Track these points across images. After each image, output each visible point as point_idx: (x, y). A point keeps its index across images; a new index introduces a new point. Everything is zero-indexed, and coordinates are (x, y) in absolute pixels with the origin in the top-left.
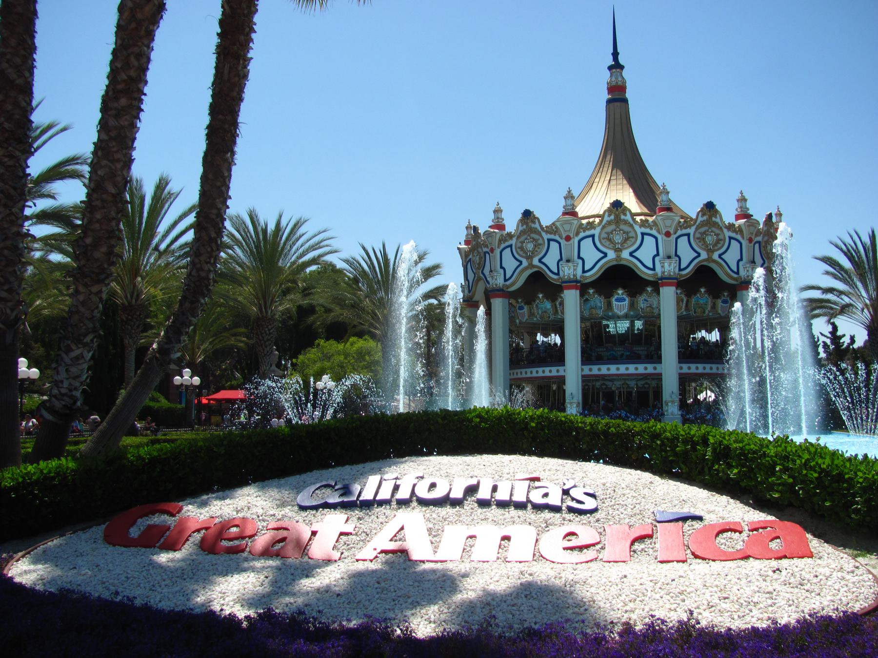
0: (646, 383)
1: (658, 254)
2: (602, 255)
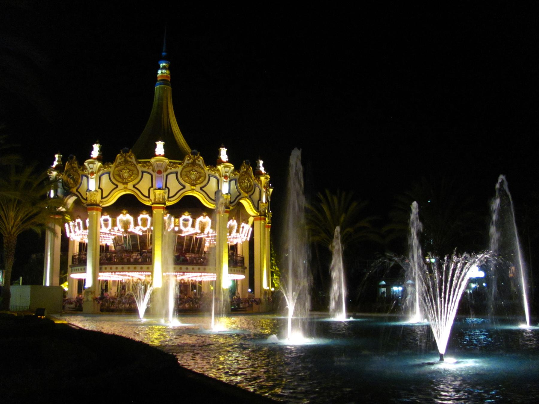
2: (182, 187)
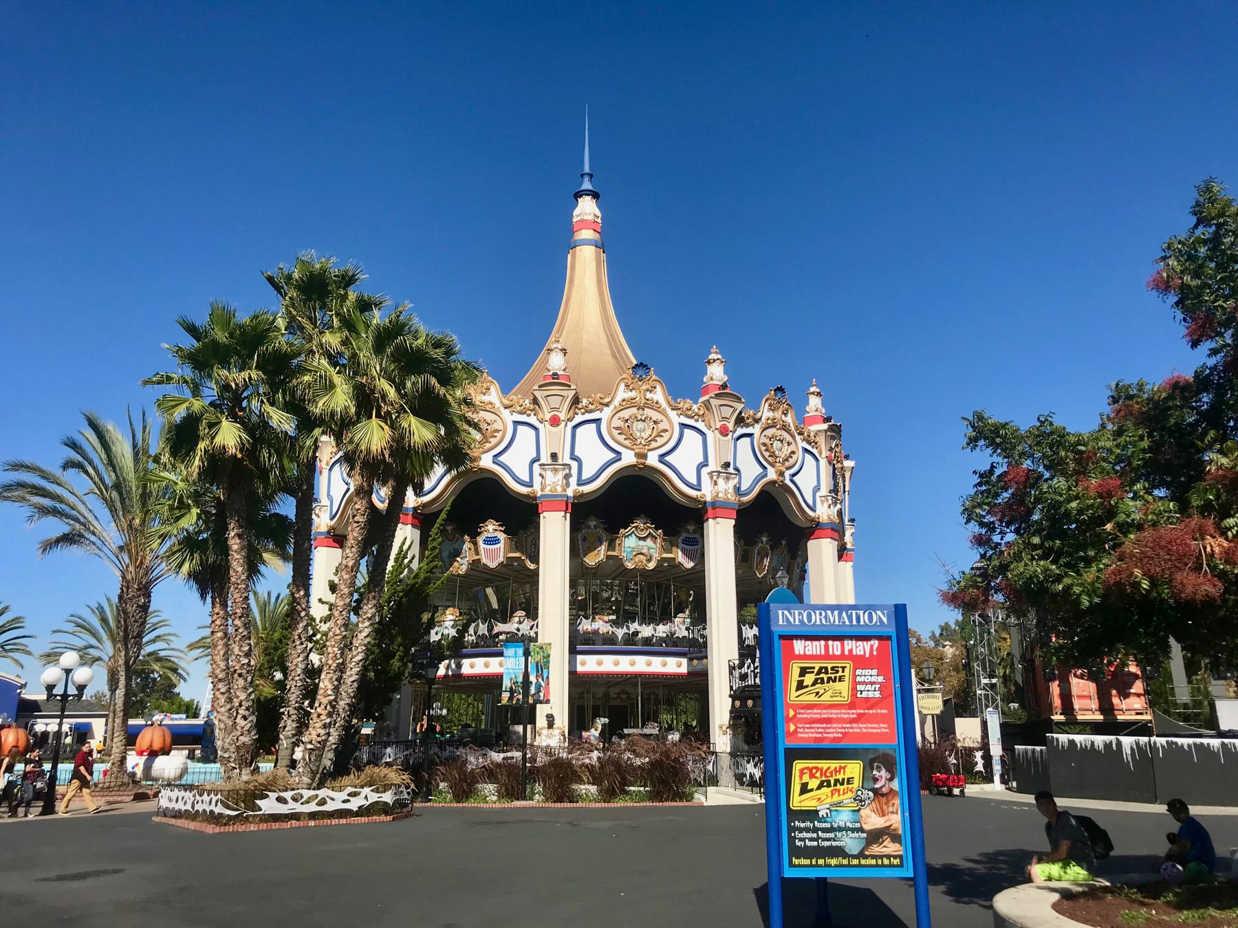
0: (623, 692)
1: (704, 464)
2: (612, 455)
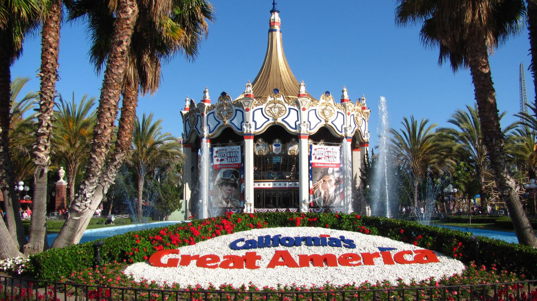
0: (289, 193)
2: (267, 120)
